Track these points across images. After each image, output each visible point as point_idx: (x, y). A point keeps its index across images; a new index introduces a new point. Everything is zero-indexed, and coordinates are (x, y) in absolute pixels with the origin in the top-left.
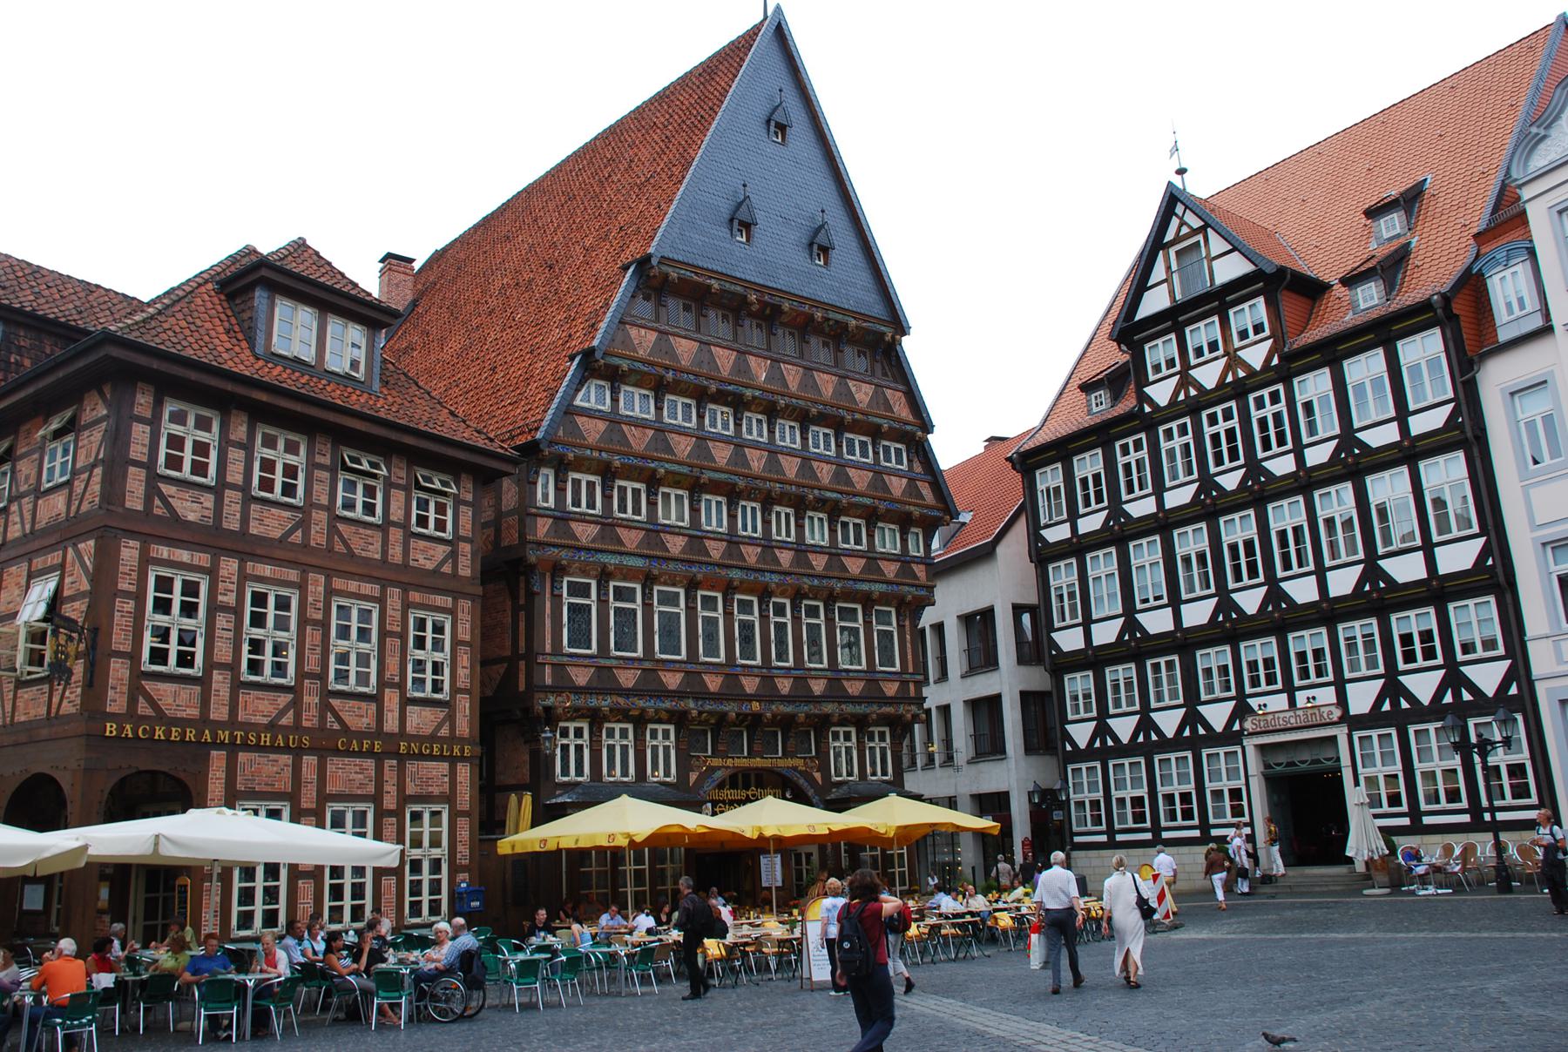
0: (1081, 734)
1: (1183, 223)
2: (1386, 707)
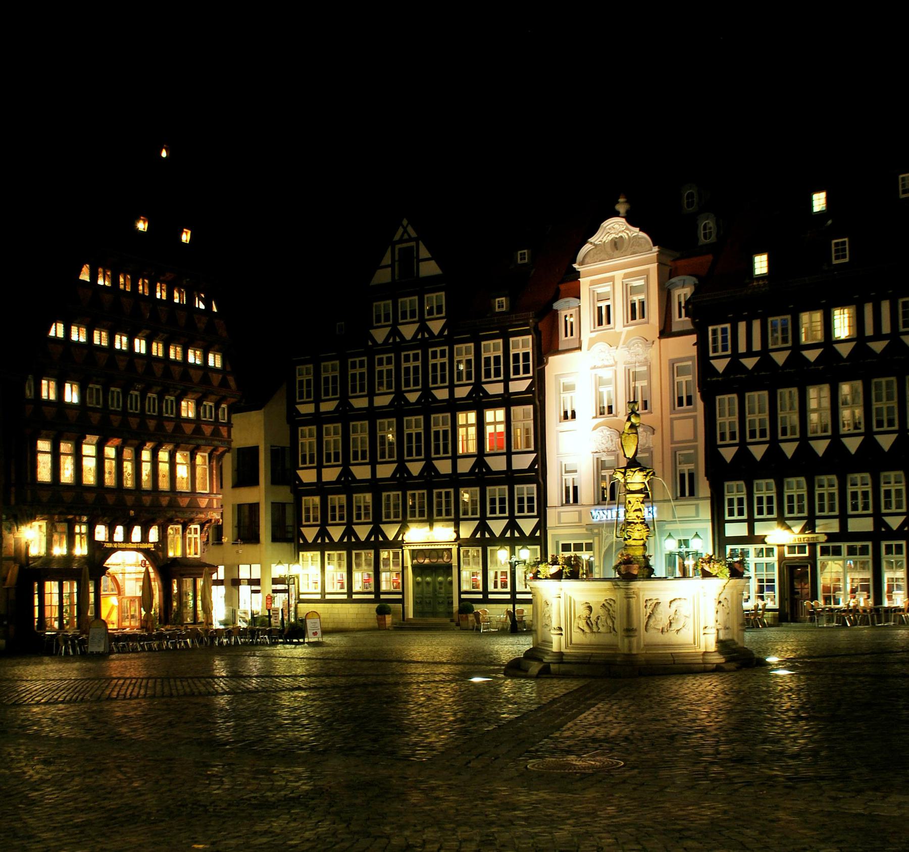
0: (310, 534)
1: (405, 231)
2: (478, 536)
